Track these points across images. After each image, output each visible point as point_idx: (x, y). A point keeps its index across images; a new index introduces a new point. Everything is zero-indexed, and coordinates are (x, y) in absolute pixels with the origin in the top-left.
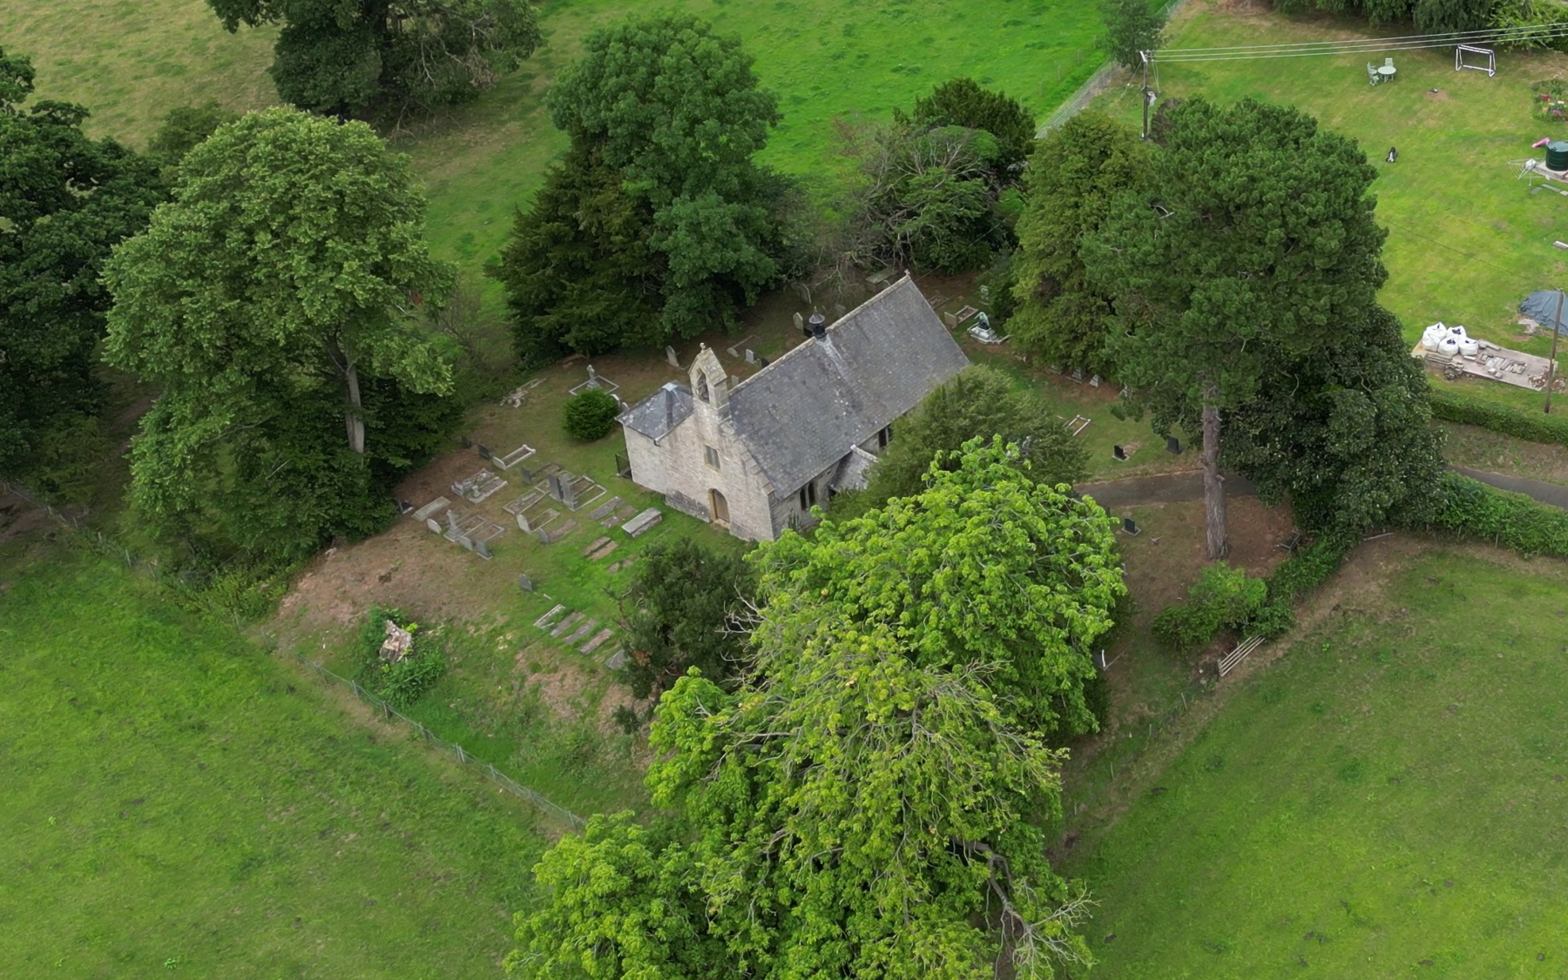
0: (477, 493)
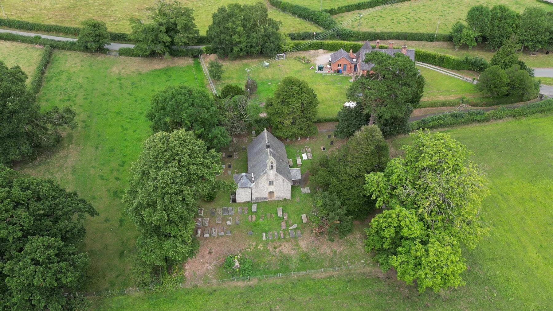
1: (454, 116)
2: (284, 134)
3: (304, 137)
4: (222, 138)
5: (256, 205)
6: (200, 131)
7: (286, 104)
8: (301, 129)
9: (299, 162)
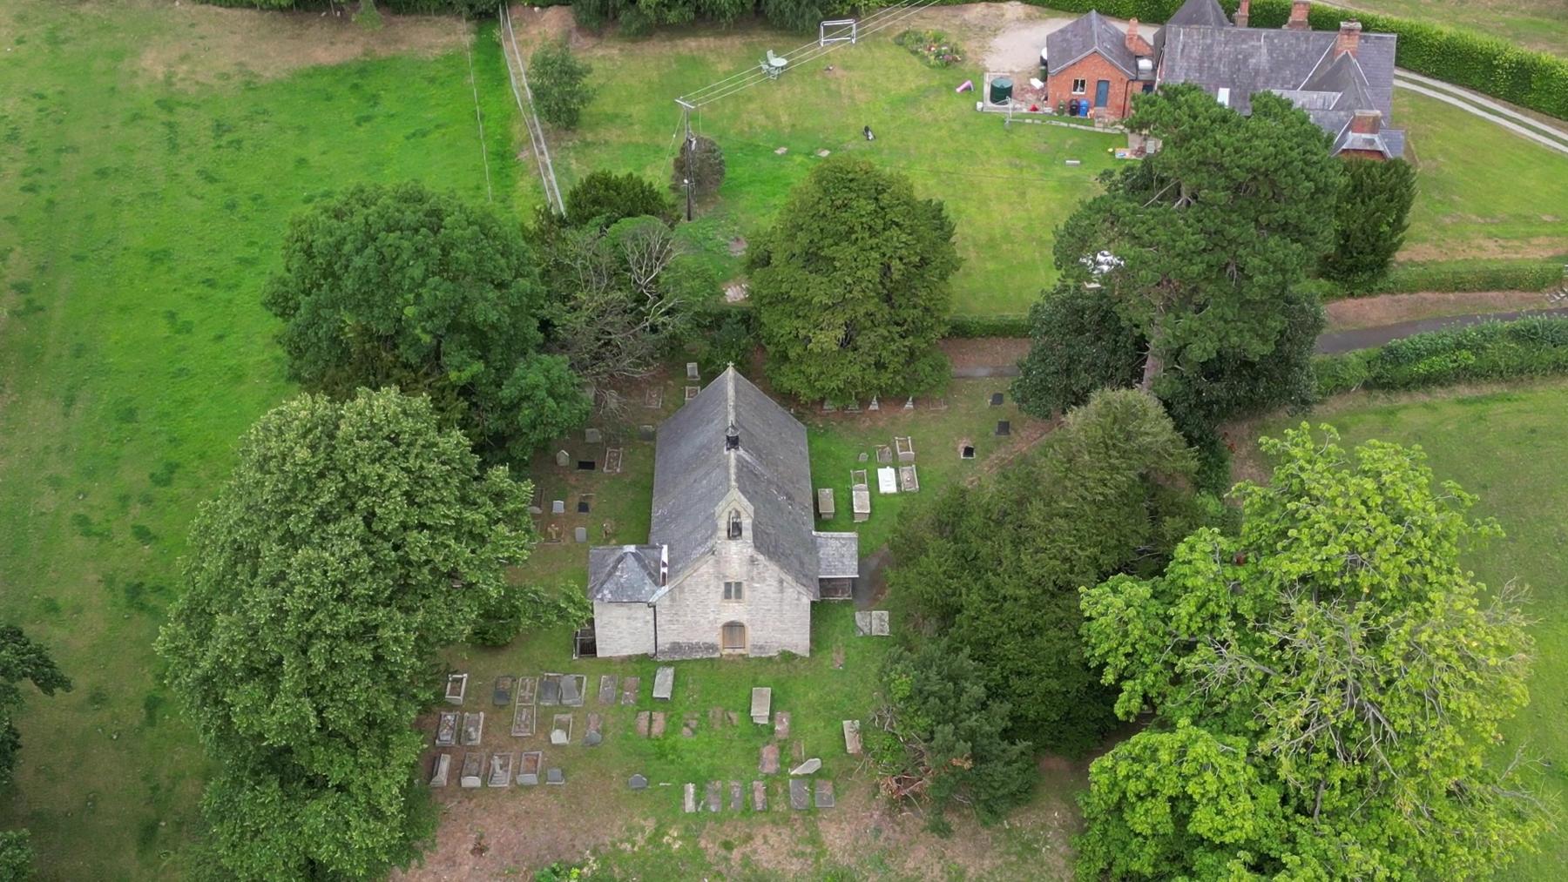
0: (474, 735)
1: (1525, 336)
2: (812, 387)
3: (892, 397)
4: (551, 402)
5: (670, 671)
6: (466, 375)
7: (822, 265)
8: (880, 366)
9: (861, 502)
